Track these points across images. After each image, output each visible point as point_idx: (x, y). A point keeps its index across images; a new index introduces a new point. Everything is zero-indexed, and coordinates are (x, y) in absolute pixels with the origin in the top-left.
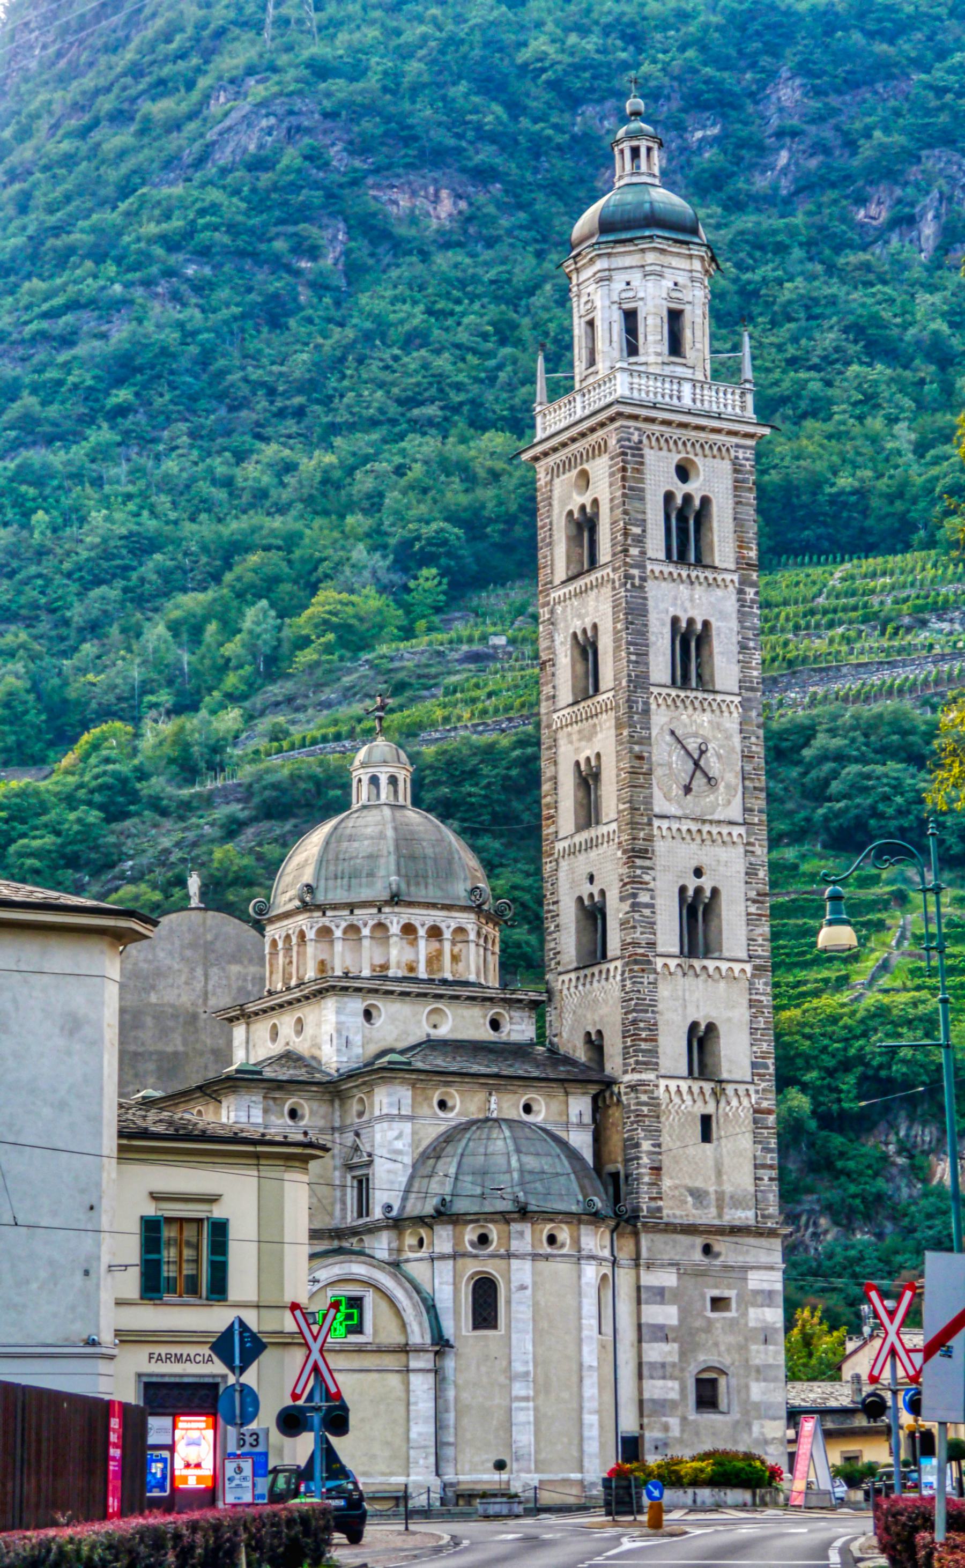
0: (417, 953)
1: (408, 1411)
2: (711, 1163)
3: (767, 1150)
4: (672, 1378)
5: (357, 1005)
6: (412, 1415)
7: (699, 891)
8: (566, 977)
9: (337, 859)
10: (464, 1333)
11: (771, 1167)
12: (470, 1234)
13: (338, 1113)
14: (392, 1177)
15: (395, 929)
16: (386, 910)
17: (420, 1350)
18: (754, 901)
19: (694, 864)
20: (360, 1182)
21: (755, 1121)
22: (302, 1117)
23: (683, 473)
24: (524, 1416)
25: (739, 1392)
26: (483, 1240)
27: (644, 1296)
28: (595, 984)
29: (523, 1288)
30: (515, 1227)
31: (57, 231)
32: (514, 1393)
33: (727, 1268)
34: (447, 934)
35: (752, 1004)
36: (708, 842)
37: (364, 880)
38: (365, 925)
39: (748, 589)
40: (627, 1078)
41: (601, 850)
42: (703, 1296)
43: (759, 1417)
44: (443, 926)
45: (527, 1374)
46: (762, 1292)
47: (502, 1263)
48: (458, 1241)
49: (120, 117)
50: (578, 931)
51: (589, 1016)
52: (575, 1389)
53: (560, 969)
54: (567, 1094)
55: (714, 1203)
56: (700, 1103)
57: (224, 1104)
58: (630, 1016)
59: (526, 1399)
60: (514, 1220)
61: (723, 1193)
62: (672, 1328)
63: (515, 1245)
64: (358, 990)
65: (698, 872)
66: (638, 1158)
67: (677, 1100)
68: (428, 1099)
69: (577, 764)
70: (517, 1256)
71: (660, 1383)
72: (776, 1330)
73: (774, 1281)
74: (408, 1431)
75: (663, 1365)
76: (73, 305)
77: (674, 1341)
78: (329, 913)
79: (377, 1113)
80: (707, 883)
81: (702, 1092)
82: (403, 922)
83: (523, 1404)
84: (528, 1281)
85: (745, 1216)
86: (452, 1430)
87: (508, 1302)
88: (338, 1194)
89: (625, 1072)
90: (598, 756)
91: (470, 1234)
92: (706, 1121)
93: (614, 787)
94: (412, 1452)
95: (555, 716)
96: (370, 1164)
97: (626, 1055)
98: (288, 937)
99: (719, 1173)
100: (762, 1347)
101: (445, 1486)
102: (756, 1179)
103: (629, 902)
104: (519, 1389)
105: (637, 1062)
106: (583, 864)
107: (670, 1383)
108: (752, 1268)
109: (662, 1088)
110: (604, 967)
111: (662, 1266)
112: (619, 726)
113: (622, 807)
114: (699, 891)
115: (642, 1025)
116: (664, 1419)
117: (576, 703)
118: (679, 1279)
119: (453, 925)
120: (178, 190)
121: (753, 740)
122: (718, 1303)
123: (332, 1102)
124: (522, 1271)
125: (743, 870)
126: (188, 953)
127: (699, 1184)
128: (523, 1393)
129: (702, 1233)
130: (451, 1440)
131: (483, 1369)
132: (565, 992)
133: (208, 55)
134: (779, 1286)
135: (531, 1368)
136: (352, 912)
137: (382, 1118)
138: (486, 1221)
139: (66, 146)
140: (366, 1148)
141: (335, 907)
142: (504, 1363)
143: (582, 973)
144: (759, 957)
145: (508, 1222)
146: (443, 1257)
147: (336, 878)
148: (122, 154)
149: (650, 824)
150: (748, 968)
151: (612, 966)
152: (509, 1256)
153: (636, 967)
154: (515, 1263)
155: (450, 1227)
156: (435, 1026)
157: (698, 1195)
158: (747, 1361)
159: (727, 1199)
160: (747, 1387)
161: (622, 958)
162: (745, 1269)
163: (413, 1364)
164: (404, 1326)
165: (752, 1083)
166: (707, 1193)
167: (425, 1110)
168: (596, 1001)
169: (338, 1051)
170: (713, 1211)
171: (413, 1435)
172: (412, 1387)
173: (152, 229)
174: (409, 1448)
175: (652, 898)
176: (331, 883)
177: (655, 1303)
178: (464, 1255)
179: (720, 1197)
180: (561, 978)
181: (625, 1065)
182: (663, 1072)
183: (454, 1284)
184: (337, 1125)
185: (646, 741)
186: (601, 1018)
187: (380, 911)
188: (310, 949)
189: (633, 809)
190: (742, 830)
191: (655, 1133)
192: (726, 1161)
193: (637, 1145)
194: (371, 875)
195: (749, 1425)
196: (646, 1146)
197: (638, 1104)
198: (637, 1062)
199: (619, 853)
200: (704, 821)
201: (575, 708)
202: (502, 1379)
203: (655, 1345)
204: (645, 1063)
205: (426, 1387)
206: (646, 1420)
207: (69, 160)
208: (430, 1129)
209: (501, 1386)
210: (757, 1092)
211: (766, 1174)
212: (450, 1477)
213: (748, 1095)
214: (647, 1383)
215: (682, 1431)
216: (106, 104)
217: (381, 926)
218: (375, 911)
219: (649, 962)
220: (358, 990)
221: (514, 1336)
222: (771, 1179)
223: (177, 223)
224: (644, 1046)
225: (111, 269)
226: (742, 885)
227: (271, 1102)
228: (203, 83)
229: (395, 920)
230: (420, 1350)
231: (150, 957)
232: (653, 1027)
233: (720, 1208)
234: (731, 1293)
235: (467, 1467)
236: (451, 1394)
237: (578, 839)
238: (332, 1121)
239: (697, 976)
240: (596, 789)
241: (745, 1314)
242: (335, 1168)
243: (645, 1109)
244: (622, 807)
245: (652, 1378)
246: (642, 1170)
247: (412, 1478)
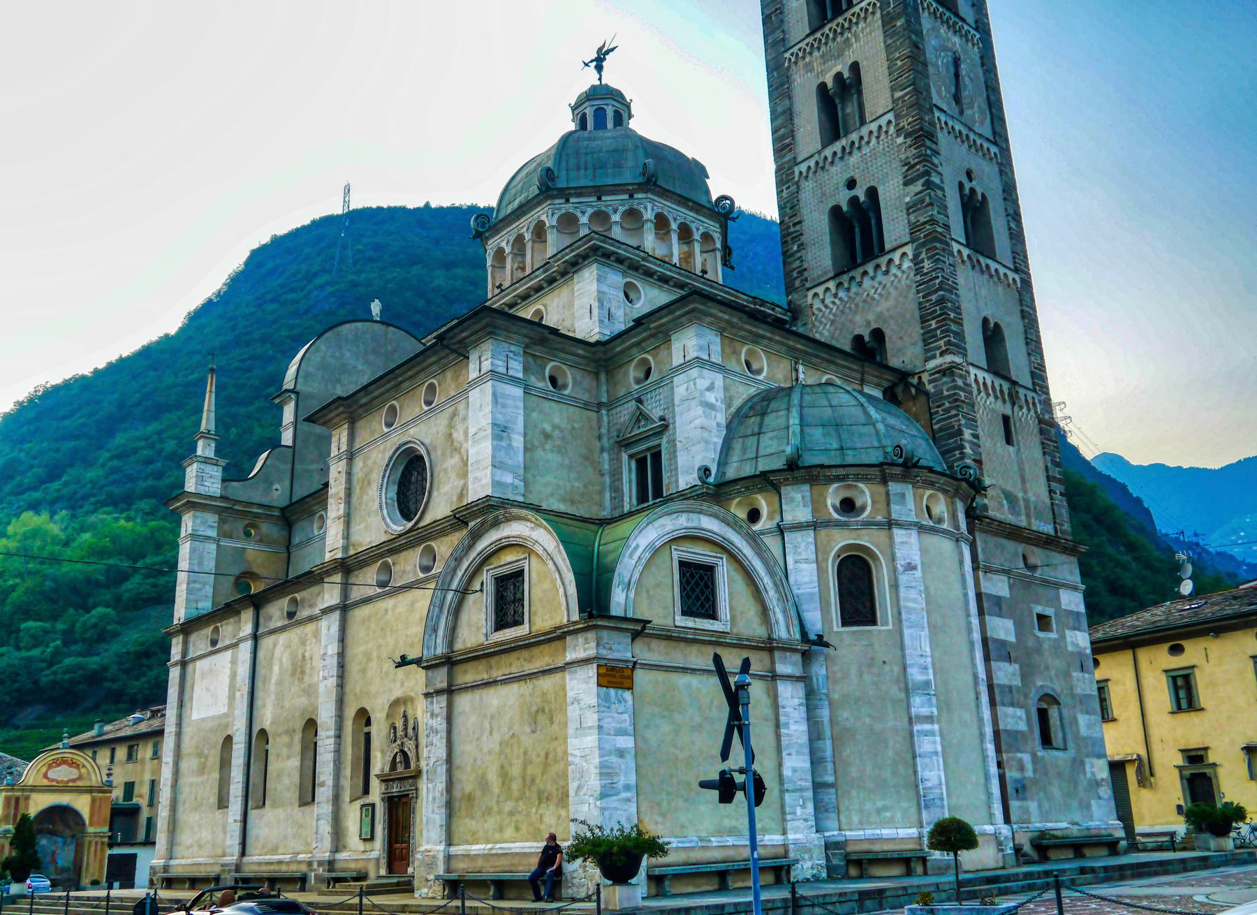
0: (670, 247)
1: (778, 736)
2: (1016, 468)
4: (1020, 706)
5: (616, 279)
6: (784, 741)
8: (820, 290)
9: (577, 153)
10: (835, 629)
12: (832, 496)
13: (604, 388)
14: (706, 435)
15: (649, 215)
16: (639, 196)
17: (787, 648)
19: (966, 165)
20: (641, 463)
21: (1041, 432)
22: (565, 386)
24: (928, 745)
25: (1071, 725)
26: (848, 506)
27: (986, 605)
28: (867, 282)
29: (910, 567)
30: (894, 487)
31: (247, 334)
32: (913, 711)
33: (1046, 583)
34: (697, 236)
36: (973, 150)
37: (610, 171)
38: (615, 211)
40: (932, 364)
41: (866, 150)
42: (1031, 612)
43: (1088, 756)
44: (693, 226)
45: (927, 684)
47: (881, 535)
48: (817, 505)
49: (272, 301)
50: (833, 243)
51: (858, 318)
52: (974, 709)
53: (808, 285)
54: (863, 382)
56: (1000, 402)
57: (474, 357)
58: (934, 298)
59: (929, 719)
60: (895, 478)
63: (897, 512)
64: (620, 260)
66: (962, 447)
67: (983, 394)
68: (736, 353)
69: (823, 86)
70: (901, 525)
72: (1087, 655)
73: (1073, 601)
74: (780, 765)
75: (1010, 688)
76: (251, 358)
77: (1016, 662)
78: (572, 200)
79: (677, 360)
81: (1001, 391)
82: (657, 210)
83: (927, 727)
84: (916, 559)
86: (830, 766)
87: (895, 586)
88: (607, 479)
89: (927, 360)
90: (855, 67)
91: (832, 496)
92: (1006, 419)
93: (885, 83)
94: (787, 796)
95: (787, 55)
96: (664, 426)
97: (928, 338)
98: (519, 240)
99: (1023, 481)
100: (1080, 674)
101: (828, 846)
103: (922, 181)
104: (920, 706)
105: (949, 343)
106: (837, 174)
109: (973, 377)
110: (883, 261)
112: (887, 21)
113: (898, 94)
114: (972, 190)
115: (949, 304)
116: (1019, 755)
117: (812, 32)
118: (1011, 587)
119: (702, 230)
120: (297, 321)
123: (597, 375)
124: (908, 545)
125: (1000, 188)
126: (371, 357)
127: (1009, 488)
128: (925, 711)
130: (830, 779)
131: (867, 677)
132: (817, 304)
133: (310, 281)
134: (1082, 609)
135: (931, 677)
136: (599, 199)
137: (686, 366)
138: (858, 478)
139: (252, 310)
140: (655, 410)
141: (580, 192)
142: (896, 669)
143: (845, 278)
145: (884, 481)
146: (798, 527)
147: (578, 169)
148: (274, 312)
149: (932, 111)
151: (896, 257)
152: (890, 524)
153: (938, 245)
154: (899, 534)
155: (806, 487)
157: (1011, 499)
158: (1072, 689)
160: (1076, 719)
161: (912, 241)
163: (782, 668)
164: (765, 612)
165: (1034, 390)
166: (1016, 497)
167: (733, 365)
168: (869, 301)
169: (601, 321)
170: (1023, 517)
171: (787, 772)
172: (781, 701)
173: (285, 333)
174: (782, 791)
175: (942, 181)
176: (573, 174)
178: (829, 524)
180: (810, 294)
181: (927, 351)
182: (969, 360)
183: (817, 561)
184: (604, 400)
185: (919, 33)
186: (880, 316)
187: (631, 196)
188: (551, 237)
189: (917, 92)
191: (972, 423)
192: (1027, 467)
193: (960, 433)
194: (618, 166)
195: (1082, 763)
196: (967, 434)
197: (956, 387)
198: (949, 343)
199: (900, 140)
200: (970, 129)
201: (818, 35)
202: (896, 692)
205: (796, 701)
206: (1005, 756)
207: (253, 314)
208: (741, 388)
209: (895, 702)
212: (833, 834)
213: (1034, 404)
214: (1001, 710)
215: (1035, 771)
216: (269, 296)
217: (633, 215)
218: (626, 197)
219: (948, 244)
220: (620, 260)
221: (907, 632)
223: (296, 331)
224: (953, 327)
225: (268, 345)
226: (1001, 200)
227: (530, 360)
228: (310, 287)
229: (649, 206)
230: (787, 648)
231: (337, 354)
232: (958, 310)
233: (1028, 516)
234: (1049, 611)
235: (855, 819)
236: (824, 713)
237: (828, 152)
238: (597, 397)
239: (982, 272)
240: (843, 109)
241: (1063, 637)
242: (602, 450)
243: (962, 394)
244: (898, 94)
245: (1003, 704)
246: (968, 461)
247: (791, 836)
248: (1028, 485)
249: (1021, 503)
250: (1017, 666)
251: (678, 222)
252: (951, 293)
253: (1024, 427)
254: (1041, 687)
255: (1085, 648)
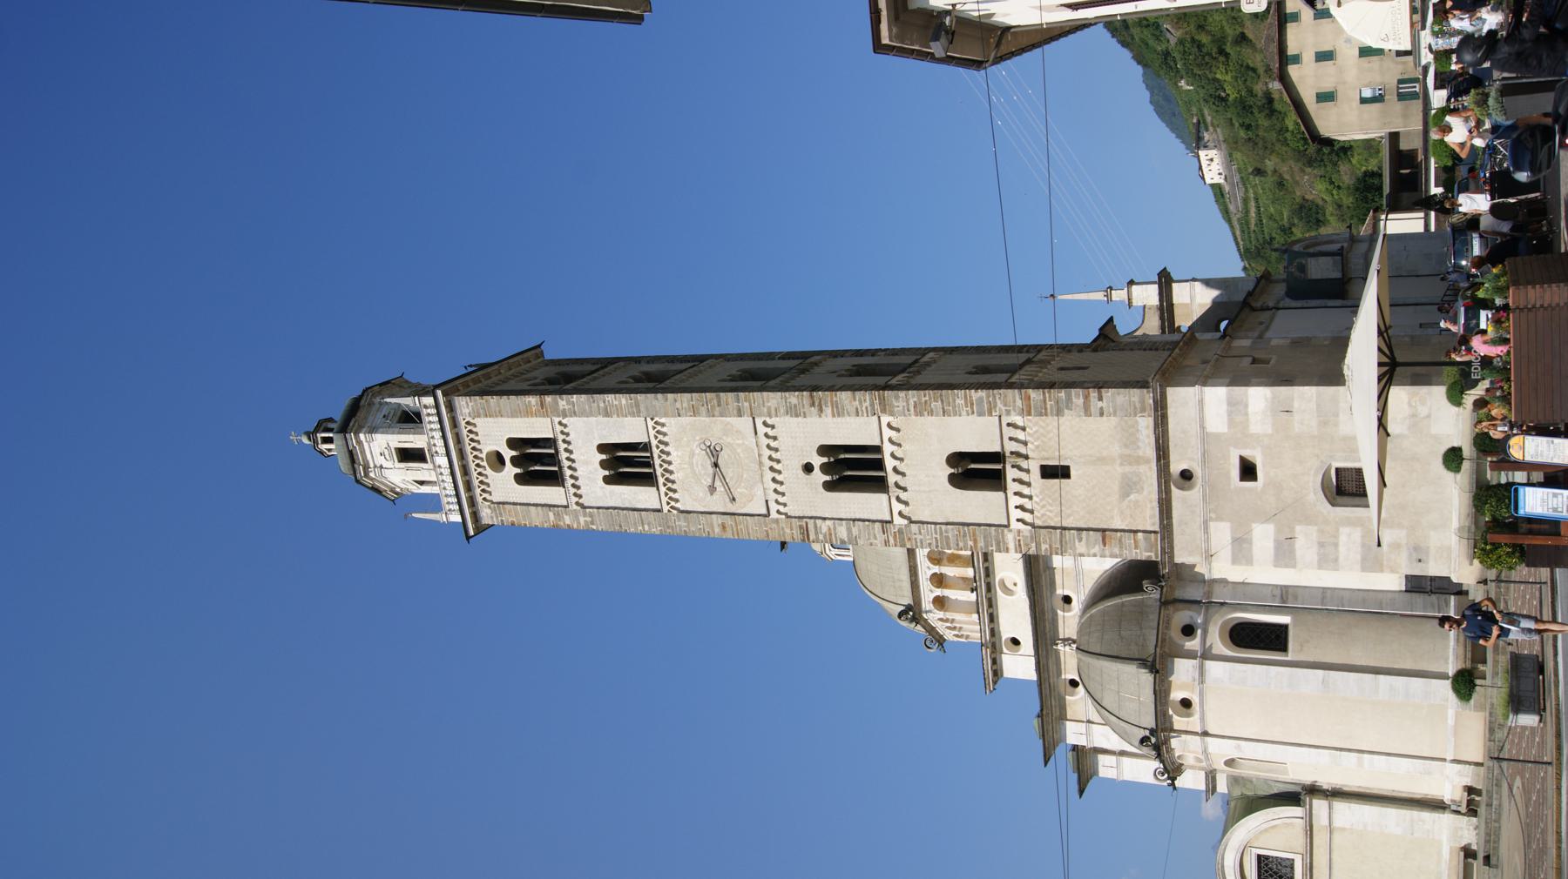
3: (1069, 399)
4: (1336, 536)
7: (825, 468)
11: (1086, 397)
18: (821, 410)
23: (498, 460)
35: (919, 413)
39: (561, 408)
46: (1230, 414)
55: (1134, 468)
61: (1121, 456)
62: (1278, 531)
64: (994, 661)
65: (808, 468)
71: (1342, 549)
75: (1321, 545)
77: (1292, 529)
80: (818, 461)
85: (1146, 424)
99: (1102, 460)
100: (1296, 417)
102: (1102, 414)
107: (1343, 539)
108: (1202, 427)
109: (1021, 526)
111: (1208, 540)
114: (825, 468)
118: (1219, 519)
121: (678, 405)
122: (1248, 471)
127: (1116, 487)
129: (1168, 492)
144: (872, 405)
150: (885, 419)
156: (1015, 584)
157: (1128, 487)
159: (1128, 452)
162: (1205, 436)
166: (1124, 476)
170: (1143, 468)
177: (1250, 550)
179: (1128, 460)
190: (759, 422)
203: (1298, 553)
204: (998, 544)
210: (1008, 413)
211: (1095, 404)
222: (1100, 399)
233: (1139, 460)
248: (1105, 453)
249: (1128, 469)
250: (1298, 528)
251: (933, 588)
252: (947, 538)
253: (1042, 441)
254: (1315, 494)
255: (1266, 399)
